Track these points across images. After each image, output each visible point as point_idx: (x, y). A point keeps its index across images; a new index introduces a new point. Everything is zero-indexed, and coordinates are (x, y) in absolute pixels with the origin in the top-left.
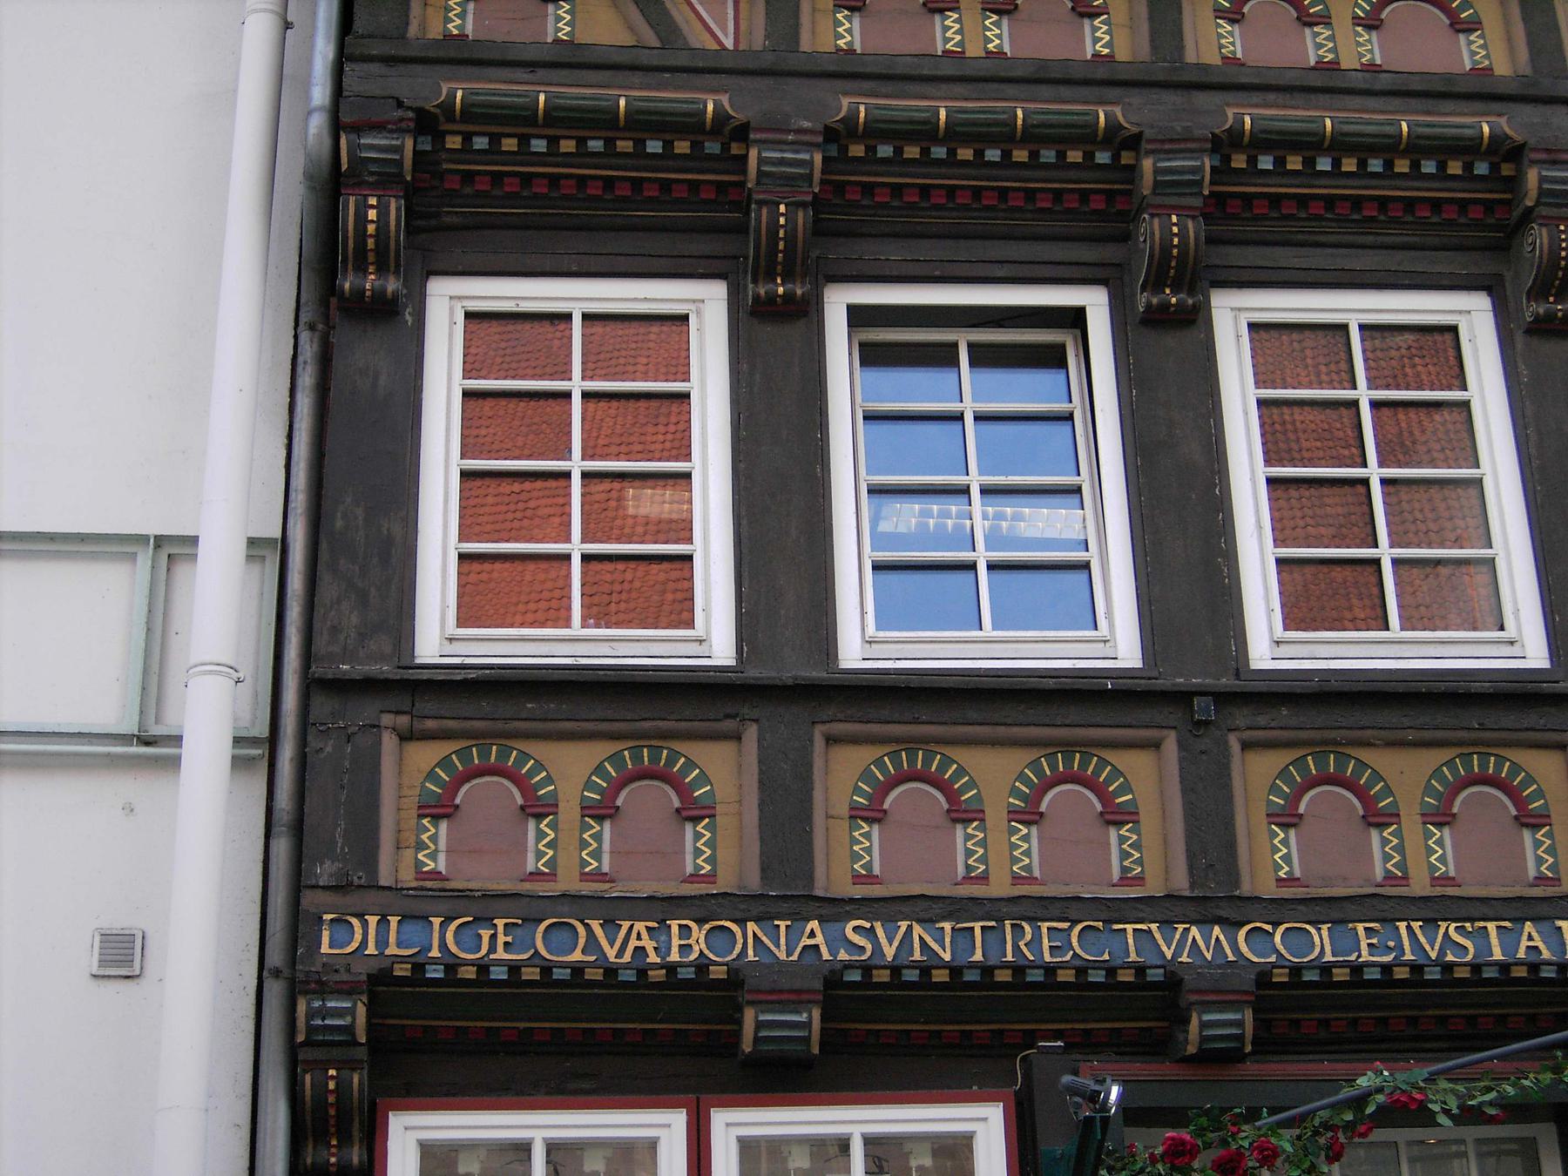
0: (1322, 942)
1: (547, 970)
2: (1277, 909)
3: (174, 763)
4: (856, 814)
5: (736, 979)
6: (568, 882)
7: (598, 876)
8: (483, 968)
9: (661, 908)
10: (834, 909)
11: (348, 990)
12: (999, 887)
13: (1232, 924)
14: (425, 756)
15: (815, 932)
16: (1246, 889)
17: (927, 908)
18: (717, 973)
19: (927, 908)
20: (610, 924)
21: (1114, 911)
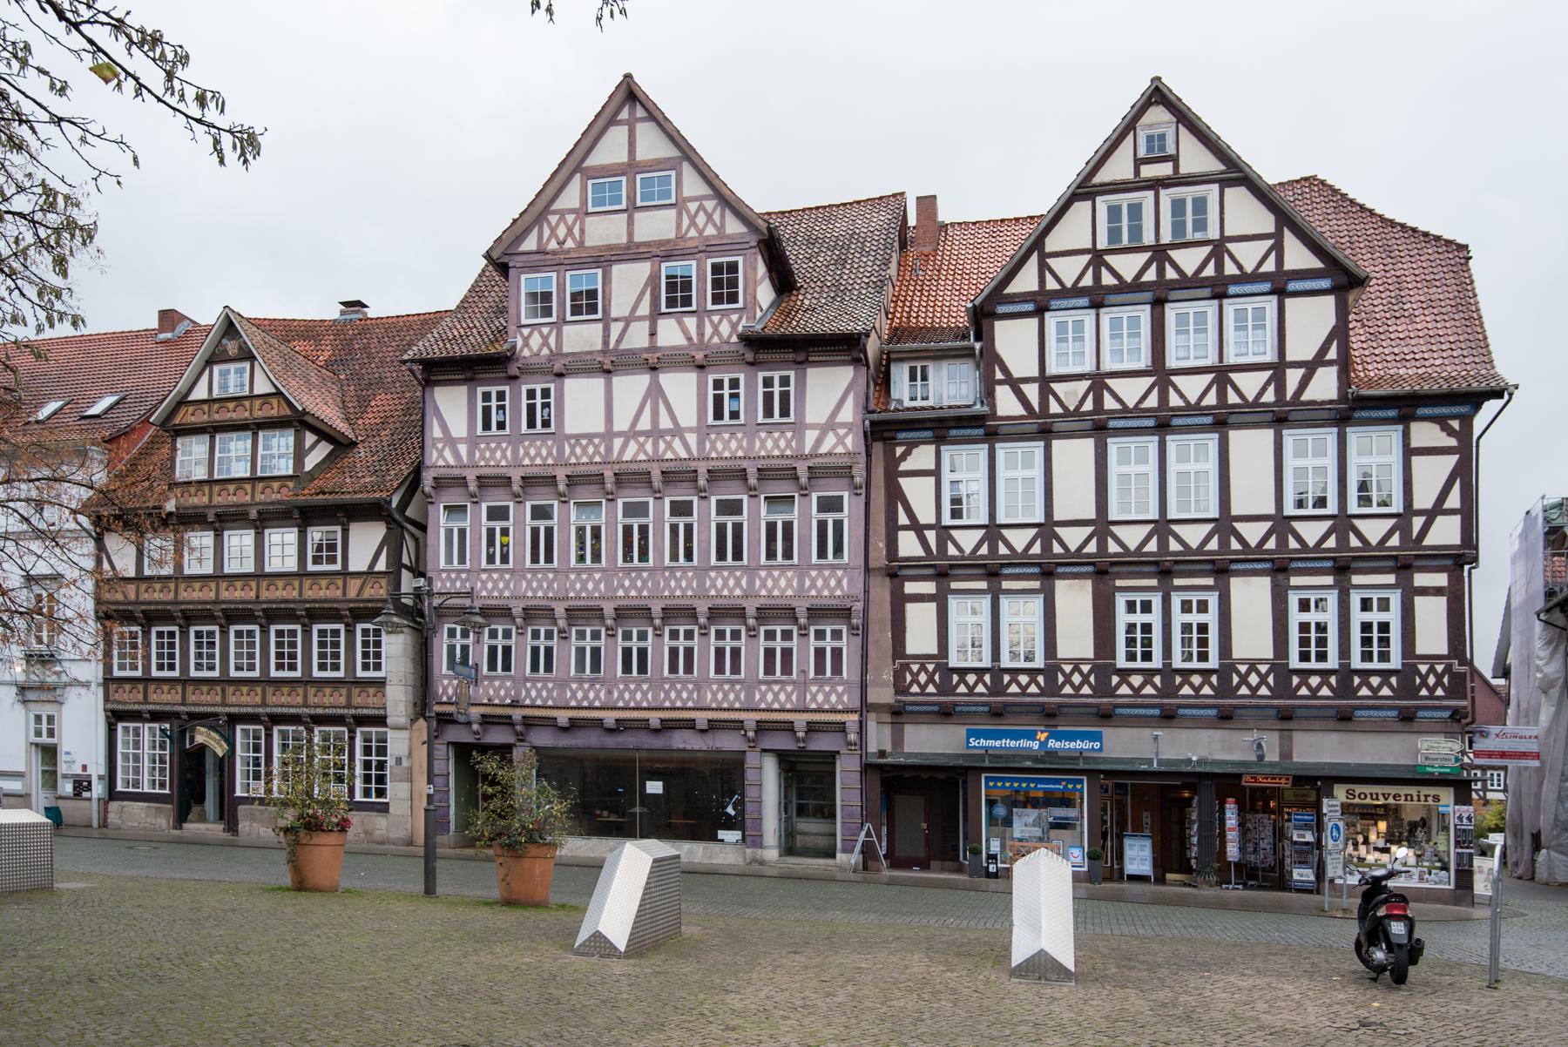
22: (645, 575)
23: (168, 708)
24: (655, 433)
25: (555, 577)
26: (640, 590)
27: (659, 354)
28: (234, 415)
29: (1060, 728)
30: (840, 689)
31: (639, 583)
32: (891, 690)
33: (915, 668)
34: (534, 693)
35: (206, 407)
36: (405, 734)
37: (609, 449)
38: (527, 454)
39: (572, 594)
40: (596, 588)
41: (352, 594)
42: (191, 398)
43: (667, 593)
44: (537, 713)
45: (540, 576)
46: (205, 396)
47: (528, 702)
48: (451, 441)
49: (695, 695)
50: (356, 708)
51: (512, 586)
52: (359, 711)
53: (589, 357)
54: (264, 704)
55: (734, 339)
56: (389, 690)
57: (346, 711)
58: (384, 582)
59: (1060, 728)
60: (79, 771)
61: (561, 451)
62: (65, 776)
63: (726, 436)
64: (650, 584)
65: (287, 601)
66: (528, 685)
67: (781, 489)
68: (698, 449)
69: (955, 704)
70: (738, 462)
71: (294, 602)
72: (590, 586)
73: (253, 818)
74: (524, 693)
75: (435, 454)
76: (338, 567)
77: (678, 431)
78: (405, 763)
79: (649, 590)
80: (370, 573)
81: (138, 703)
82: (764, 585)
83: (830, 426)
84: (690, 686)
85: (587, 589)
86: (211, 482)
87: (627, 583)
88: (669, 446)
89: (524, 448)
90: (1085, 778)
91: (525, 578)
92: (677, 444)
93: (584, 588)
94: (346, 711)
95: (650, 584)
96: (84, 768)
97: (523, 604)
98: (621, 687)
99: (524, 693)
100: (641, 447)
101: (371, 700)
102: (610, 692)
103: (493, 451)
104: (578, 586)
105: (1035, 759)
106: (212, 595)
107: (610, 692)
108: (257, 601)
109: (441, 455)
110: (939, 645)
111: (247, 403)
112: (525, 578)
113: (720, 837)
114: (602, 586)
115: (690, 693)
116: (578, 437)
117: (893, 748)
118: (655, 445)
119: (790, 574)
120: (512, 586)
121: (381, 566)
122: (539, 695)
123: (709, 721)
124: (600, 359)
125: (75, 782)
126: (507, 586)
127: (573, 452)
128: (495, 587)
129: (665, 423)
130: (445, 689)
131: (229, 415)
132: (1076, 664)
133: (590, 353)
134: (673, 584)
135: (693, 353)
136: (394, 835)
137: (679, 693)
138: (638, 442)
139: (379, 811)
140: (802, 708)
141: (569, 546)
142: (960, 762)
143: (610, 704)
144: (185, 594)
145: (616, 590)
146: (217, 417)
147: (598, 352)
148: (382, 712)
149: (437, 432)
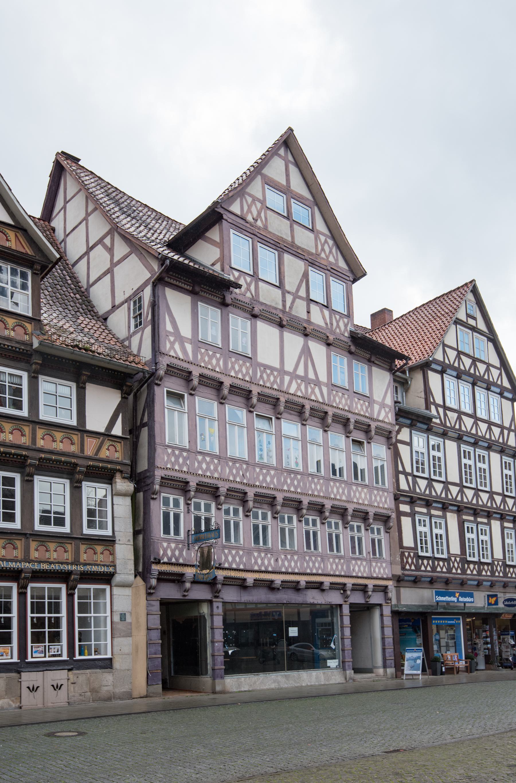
22: (299, 477)
24: (305, 379)
25: (247, 468)
26: (296, 487)
27: (312, 327)
29: (450, 590)
30: (384, 565)
31: (296, 483)
32: (399, 567)
33: (406, 554)
34: (230, 559)
36: (127, 591)
37: (282, 381)
38: (233, 368)
39: (257, 483)
40: (272, 481)
41: (89, 451)
43: (310, 492)
44: (233, 574)
45: (238, 465)
47: (226, 565)
48: (181, 340)
49: (322, 565)
50: (85, 564)
51: (219, 469)
52: (88, 568)
53: (274, 311)
55: (346, 334)
57: (74, 567)
58: (118, 446)
59: (450, 590)
61: (255, 373)
63: (340, 394)
64: (301, 484)
65: (18, 447)
66: (226, 551)
67: (359, 436)
68: (328, 399)
69: (422, 576)
70: (347, 414)
71: (27, 449)
72: (268, 479)
74: (223, 558)
75: (168, 345)
77: (317, 383)
78: (129, 619)
79: (301, 489)
80: (107, 435)
82: (355, 495)
83: (383, 405)
84: (319, 559)
85: (266, 481)
87: (289, 481)
88: (313, 392)
89: (232, 363)
90: (461, 617)
91: (228, 465)
92: (317, 390)
93: (265, 480)
94: (74, 567)
95: (301, 484)
97: (227, 485)
98: (283, 557)
99: (223, 558)
100: (299, 388)
101: (100, 558)
102: (277, 560)
103: (211, 358)
104: (261, 478)
105: (444, 608)
107: (277, 560)
109: (172, 347)
110: (414, 543)
112: (228, 465)
113: (328, 665)
114: (275, 480)
115: (320, 564)
116: (266, 367)
117: (397, 602)
118: (306, 388)
119: (365, 490)
120: (219, 469)
121: (117, 430)
122: (234, 560)
123: (331, 583)
124: (281, 316)
126: (216, 470)
127: (261, 377)
128: (208, 468)
129: (311, 375)
130: (165, 551)
132: (456, 556)
133: (276, 309)
134: (313, 486)
135: (328, 335)
137: (314, 563)
138: (297, 382)
139: (101, 667)
140: (370, 576)
141: (254, 445)
142: (421, 610)
143: (277, 570)
145: (283, 485)
147: (280, 309)
148: (111, 569)
149: (169, 327)
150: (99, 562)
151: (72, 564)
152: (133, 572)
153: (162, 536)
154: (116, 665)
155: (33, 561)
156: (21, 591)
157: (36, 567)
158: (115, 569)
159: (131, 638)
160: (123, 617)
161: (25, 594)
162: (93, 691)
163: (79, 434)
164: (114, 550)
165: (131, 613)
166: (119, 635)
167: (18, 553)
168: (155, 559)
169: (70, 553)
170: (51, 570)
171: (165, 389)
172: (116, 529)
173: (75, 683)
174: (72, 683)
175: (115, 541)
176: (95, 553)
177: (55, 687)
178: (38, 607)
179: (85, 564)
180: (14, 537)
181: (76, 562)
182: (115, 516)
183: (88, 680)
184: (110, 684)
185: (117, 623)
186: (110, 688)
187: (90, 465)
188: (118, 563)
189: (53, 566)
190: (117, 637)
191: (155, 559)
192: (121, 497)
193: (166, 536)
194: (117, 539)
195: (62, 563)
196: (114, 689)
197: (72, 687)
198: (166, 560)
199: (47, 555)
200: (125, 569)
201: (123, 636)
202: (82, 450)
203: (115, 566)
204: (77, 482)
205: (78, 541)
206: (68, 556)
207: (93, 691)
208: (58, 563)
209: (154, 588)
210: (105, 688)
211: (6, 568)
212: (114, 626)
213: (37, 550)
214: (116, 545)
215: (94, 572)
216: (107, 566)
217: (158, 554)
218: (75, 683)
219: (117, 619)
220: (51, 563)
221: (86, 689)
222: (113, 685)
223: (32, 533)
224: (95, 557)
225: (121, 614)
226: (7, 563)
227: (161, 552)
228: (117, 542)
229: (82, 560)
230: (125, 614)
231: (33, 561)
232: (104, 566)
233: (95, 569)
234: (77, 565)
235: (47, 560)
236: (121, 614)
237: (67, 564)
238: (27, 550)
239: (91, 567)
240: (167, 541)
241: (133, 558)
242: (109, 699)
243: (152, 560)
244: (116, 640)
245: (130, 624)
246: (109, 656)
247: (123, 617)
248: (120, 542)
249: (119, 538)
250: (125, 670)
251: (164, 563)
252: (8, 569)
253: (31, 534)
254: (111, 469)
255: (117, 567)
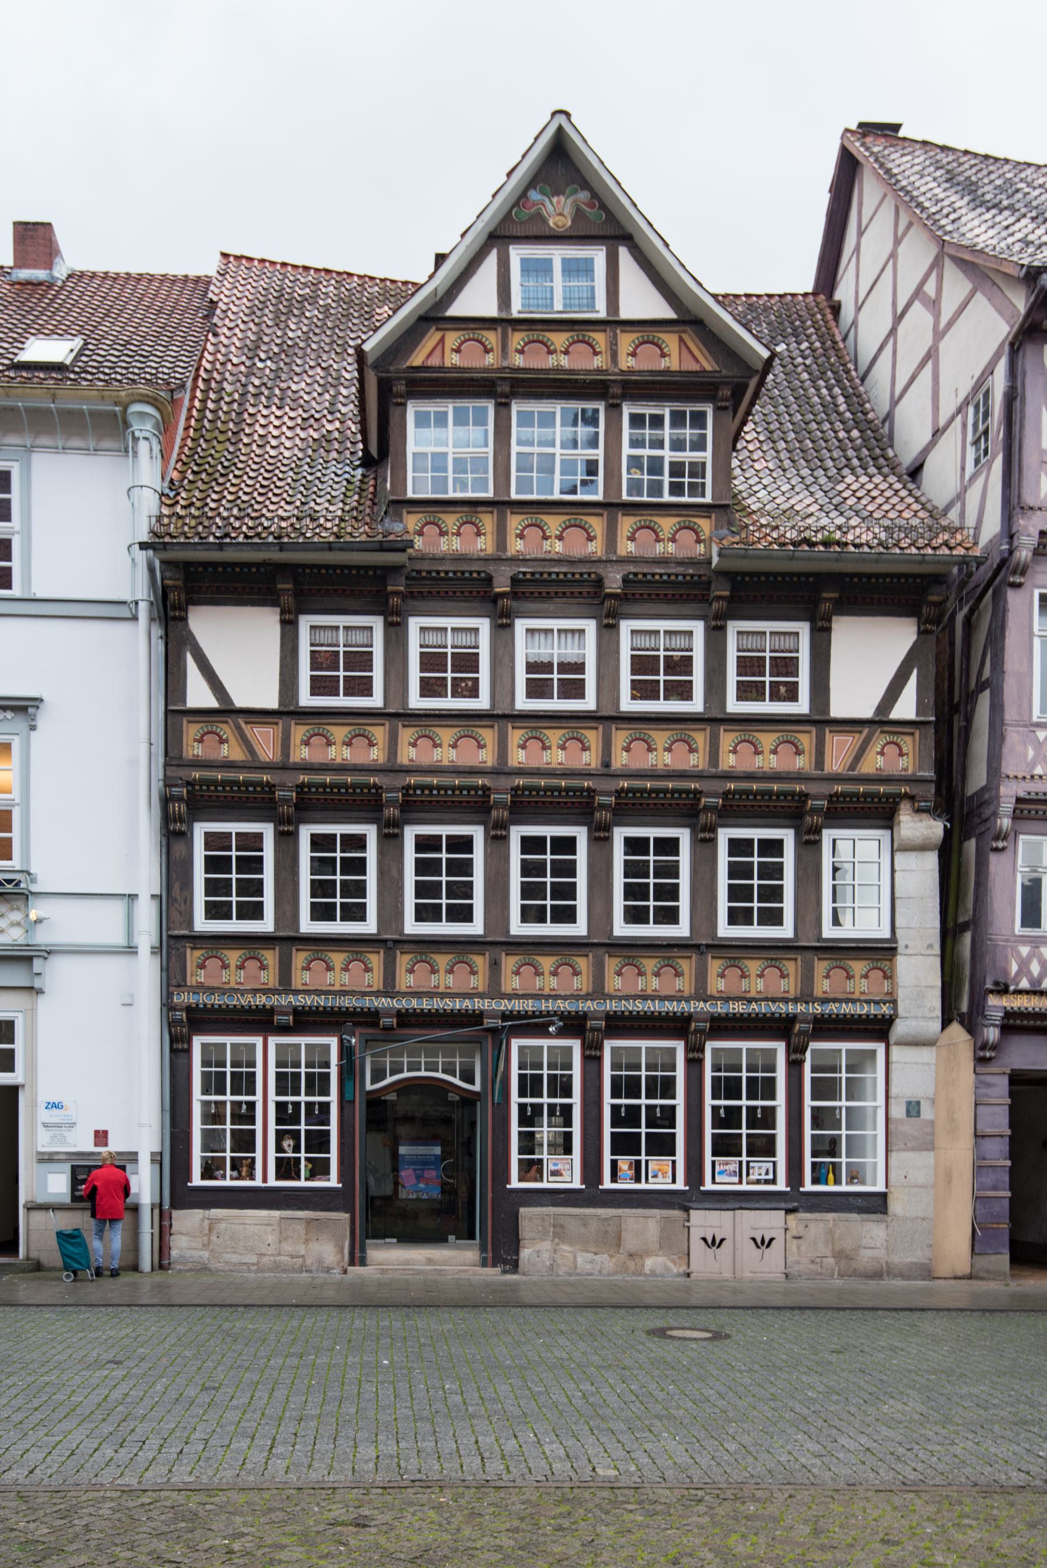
0: (414, 1003)
1: (227, 1006)
2: (404, 995)
3: (136, 953)
4: (303, 969)
5: (272, 1008)
6: (233, 985)
7: (240, 983)
8: (212, 1005)
9: (255, 992)
10: (296, 992)
11: (181, 1010)
12: (337, 988)
13: (392, 998)
14: (198, 953)
15: (291, 998)
16: (397, 989)
17: (318, 993)
18: (268, 1007)
19: (318, 993)
20: (242, 995)
21: (364, 994)
23: (347, 1002)
28: (565, 362)
35: (492, 338)
42: (456, 310)
46: (490, 309)
50: (824, 1001)
52: (832, 1008)
54: (598, 992)
56: (903, 964)
57: (800, 1008)
58: (907, 743)
60: (87, 1145)
62: (47, 1159)
65: (682, 775)
71: (699, 776)
73: (560, 1233)
76: (802, 706)
81: (266, 992)
86: (501, 505)
94: (800, 1008)
96: (101, 1137)
101: (860, 986)
106: (376, 755)
108: (501, 771)
111: (600, 339)
121: (906, 708)
125: (74, 1168)
130: (1024, 965)
131: (551, 362)
136: (902, 1258)
139: (861, 1210)
144: (412, 752)
146: (519, 361)
148: (886, 1010)
150: (856, 996)
151: (795, 1001)
152: (938, 1013)
153: (1017, 932)
154: (895, 1206)
155: (712, 998)
156: (691, 1055)
157: (720, 1008)
158: (895, 1009)
159: (932, 1154)
160: (913, 1109)
161: (700, 1061)
162: (840, 1255)
163: (814, 730)
164: (893, 968)
165: (933, 1101)
166: (903, 1146)
167: (684, 984)
168: (996, 983)
169: (792, 978)
170: (750, 1014)
171: (1036, 593)
172: (898, 923)
173: (800, 1238)
174: (795, 1238)
175: (895, 949)
176: (849, 977)
177: (759, 1241)
178: (728, 1088)
179: (824, 1001)
180: (676, 952)
181: (806, 996)
182: (897, 895)
183: (830, 1232)
184: (879, 1245)
185: (900, 1121)
186: (881, 1253)
187: (836, 793)
188: (901, 995)
189: (754, 1006)
190: (899, 1150)
191: (996, 983)
192: (913, 854)
193: (1029, 932)
194: (901, 945)
195: (774, 1000)
196: (888, 1254)
197: (793, 1245)
198: (1024, 984)
199: (744, 984)
200: (920, 1007)
201: (913, 1149)
202: (820, 763)
203: (894, 1002)
204: (809, 832)
205: (808, 955)
206: (790, 986)
207: (840, 1255)
208: (766, 999)
209: (994, 1047)
210: (869, 1253)
211: (660, 1013)
212: (892, 1127)
213: (722, 975)
214: (899, 958)
215: (845, 1015)
216: (877, 1003)
217: (1006, 972)
218: (800, 1238)
219: (898, 1111)
220: (750, 1001)
221: (824, 1250)
222: (887, 1248)
223: (710, 942)
224: (849, 986)
225: (909, 1103)
226: (662, 1003)
227: (1014, 968)
228: (899, 950)
229: (818, 992)
230: (918, 1103)
231: (712, 998)
232: (868, 1002)
233: (846, 1009)
234: (807, 1003)
235: (743, 995)
236: (909, 1103)
237: (786, 1001)
238: (701, 977)
239: (837, 1005)
240: (1031, 942)
241: (939, 983)
242: (878, 1275)
243: (989, 986)
244: (894, 1157)
245: (932, 1123)
246: (880, 1188)
247: (913, 1109)
248: (908, 951)
249: (907, 942)
250: (916, 1218)
251: (1020, 992)
252: (663, 1014)
253: (708, 946)
254: (887, 795)
255: (900, 1003)
